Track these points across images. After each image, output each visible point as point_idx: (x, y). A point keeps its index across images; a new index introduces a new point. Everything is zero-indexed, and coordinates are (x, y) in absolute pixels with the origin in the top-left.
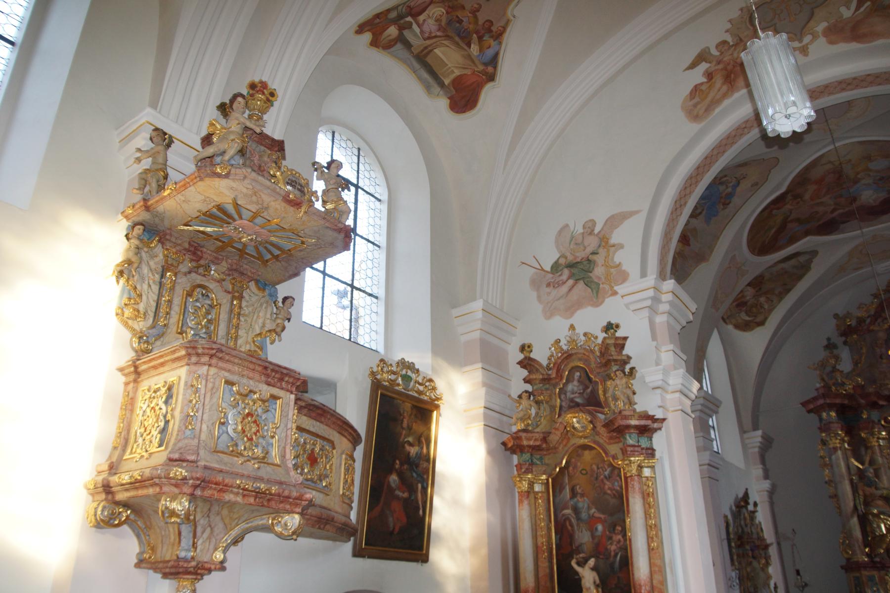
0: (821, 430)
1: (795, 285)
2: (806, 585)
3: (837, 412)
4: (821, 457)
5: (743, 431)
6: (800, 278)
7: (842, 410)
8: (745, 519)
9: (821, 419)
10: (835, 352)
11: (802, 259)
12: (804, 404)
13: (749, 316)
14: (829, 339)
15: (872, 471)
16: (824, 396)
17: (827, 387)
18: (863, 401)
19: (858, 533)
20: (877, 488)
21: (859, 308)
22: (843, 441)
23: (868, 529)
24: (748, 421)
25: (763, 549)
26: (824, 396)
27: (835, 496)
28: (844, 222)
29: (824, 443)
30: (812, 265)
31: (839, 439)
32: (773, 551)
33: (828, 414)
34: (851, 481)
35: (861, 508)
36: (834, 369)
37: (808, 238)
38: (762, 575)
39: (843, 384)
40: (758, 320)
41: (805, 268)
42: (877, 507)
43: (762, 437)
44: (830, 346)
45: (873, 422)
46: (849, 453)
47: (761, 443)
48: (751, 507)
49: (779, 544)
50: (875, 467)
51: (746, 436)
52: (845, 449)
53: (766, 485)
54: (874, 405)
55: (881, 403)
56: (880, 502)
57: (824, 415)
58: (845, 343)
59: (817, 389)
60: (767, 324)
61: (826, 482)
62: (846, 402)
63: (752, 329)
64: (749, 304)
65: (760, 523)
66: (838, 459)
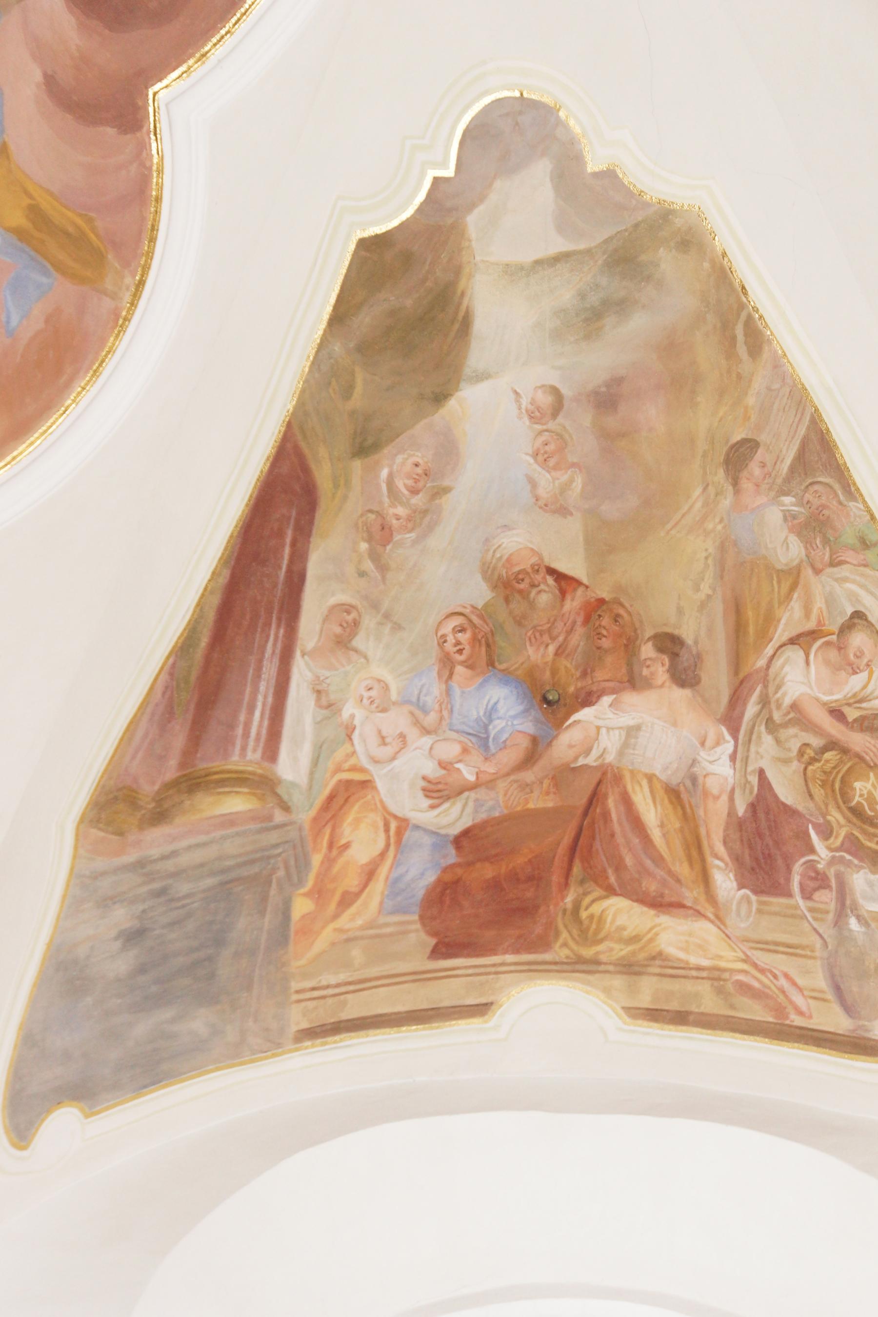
1: (800, 397)
64: (786, 791)
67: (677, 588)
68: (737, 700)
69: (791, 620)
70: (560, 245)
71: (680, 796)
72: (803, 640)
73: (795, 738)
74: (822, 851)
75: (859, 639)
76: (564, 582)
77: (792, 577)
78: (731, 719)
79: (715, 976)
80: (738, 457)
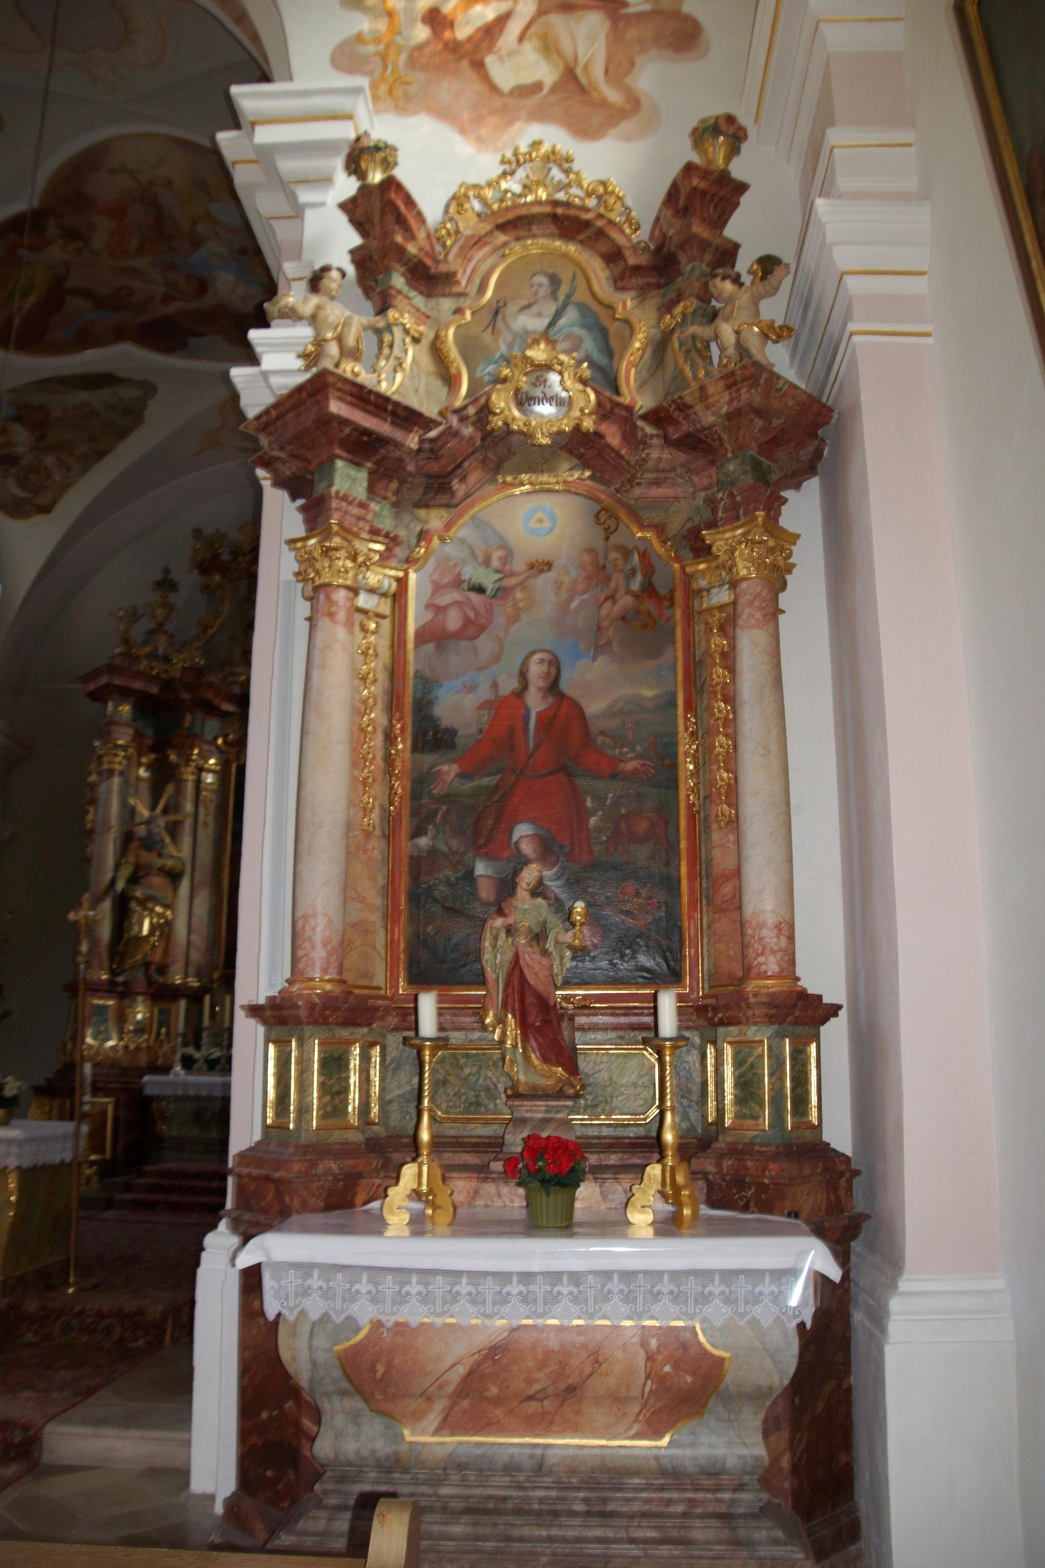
6: (122, 434)
7: (144, 704)
14: (167, 571)
18: (185, 696)
20: (160, 855)
30: (148, 414)
40: (42, 500)
41: (130, 418)
62: (155, 690)
63: (28, 517)
66: (109, 791)
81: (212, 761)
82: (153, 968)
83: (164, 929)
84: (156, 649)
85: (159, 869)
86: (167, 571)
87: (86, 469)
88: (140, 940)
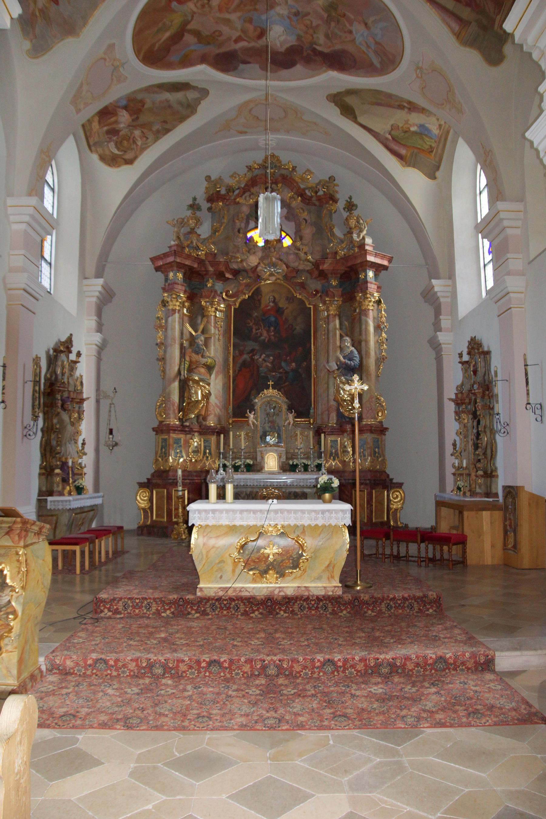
0: (164, 290)
1: (175, 127)
2: (116, 444)
3: (184, 275)
4: (158, 317)
5: (83, 276)
6: (182, 119)
8: (63, 367)
9: (166, 279)
10: (198, 213)
11: (191, 95)
12: (153, 260)
13: (118, 149)
14: (195, 199)
15: (203, 338)
16: (175, 253)
17: (181, 247)
18: (211, 269)
19: (175, 397)
20: (203, 356)
21: (231, 176)
22: (183, 304)
23: (186, 395)
24: (91, 268)
25: (77, 403)
26: (175, 253)
27: (163, 359)
28: (245, 62)
29: (164, 303)
30: (199, 109)
31: (179, 301)
32: (89, 407)
33: (175, 274)
34: (181, 345)
35: (184, 373)
36: (192, 231)
37: (202, 67)
38: (70, 428)
39: (197, 248)
40: (127, 157)
41: (191, 108)
42: (200, 374)
43: (102, 286)
44: (194, 207)
45: (216, 292)
46: (186, 319)
47: (100, 292)
48: (73, 357)
49: (98, 401)
50: (207, 336)
51: (85, 282)
52: (183, 313)
53: (97, 338)
54: (220, 276)
55: (228, 275)
56: (203, 370)
57: (171, 274)
58: (209, 209)
59: (170, 247)
60: (136, 163)
61: (157, 344)
62: (196, 266)
63: (119, 166)
64: (121, 133)
65: (81, 376)
67: (145, 118)
68: (132, 126)
69: (145, 131)
70: (189, 99)
71: (116, 122)
72: (142, 132)
73: (129, 134)
74: (115, 138)
75: (145, 139)
76: (143, 106)
77: (151, 130)
78: (129, 126)
79: (91, 129)
80: (165, 122)
81: (222, 306)
82: (201, 418)
83: (207, 397)
84: (192, 242)
85: (204, 364)
86: (195, 199)
87: (157, 139)
88: (198, 402)
